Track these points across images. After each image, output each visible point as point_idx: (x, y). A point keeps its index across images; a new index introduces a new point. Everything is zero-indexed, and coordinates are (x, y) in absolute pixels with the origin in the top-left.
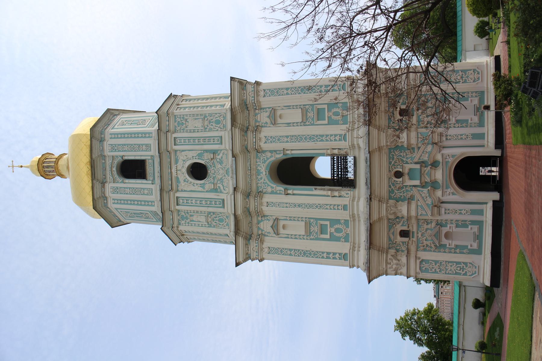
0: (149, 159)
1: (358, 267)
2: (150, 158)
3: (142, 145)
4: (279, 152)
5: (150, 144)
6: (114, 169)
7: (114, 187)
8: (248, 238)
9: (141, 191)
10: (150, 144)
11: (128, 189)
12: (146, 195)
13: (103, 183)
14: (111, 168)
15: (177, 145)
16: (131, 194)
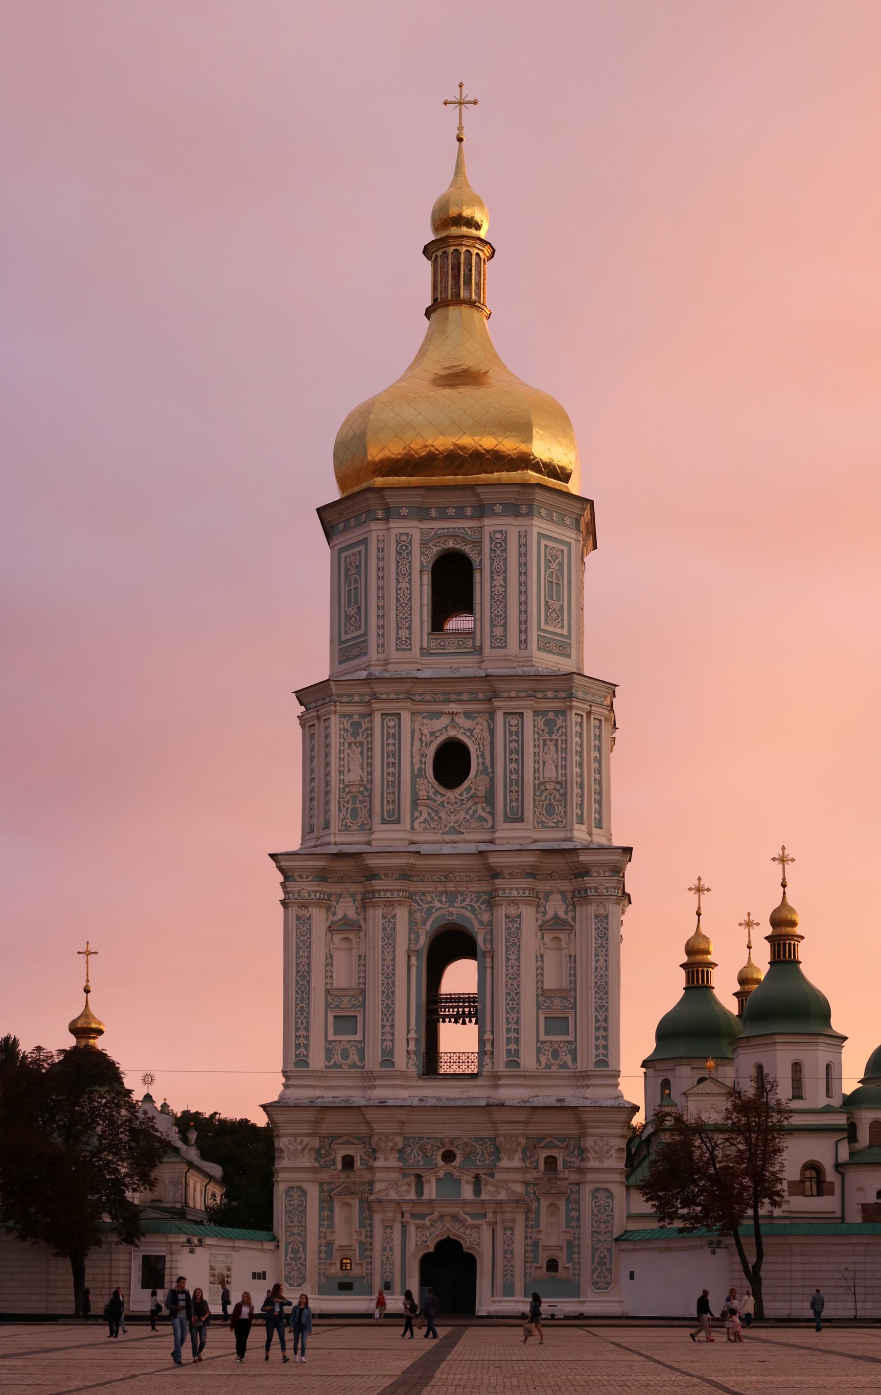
0: (474, 639)
1: (286, 1086)
2: (478, 644)
3: (505, 626)
4: (488, 940)
5: (505, 647)
6: (451, 544)
7: (410, 542)
8: (322, 876)
9: (404, 619)
10: (505, 647)
11: (408, 586)
12: (397, 633)
13: (421, 513)
14: (454, 537)
15: (505, 719)
16: (397, 594)
